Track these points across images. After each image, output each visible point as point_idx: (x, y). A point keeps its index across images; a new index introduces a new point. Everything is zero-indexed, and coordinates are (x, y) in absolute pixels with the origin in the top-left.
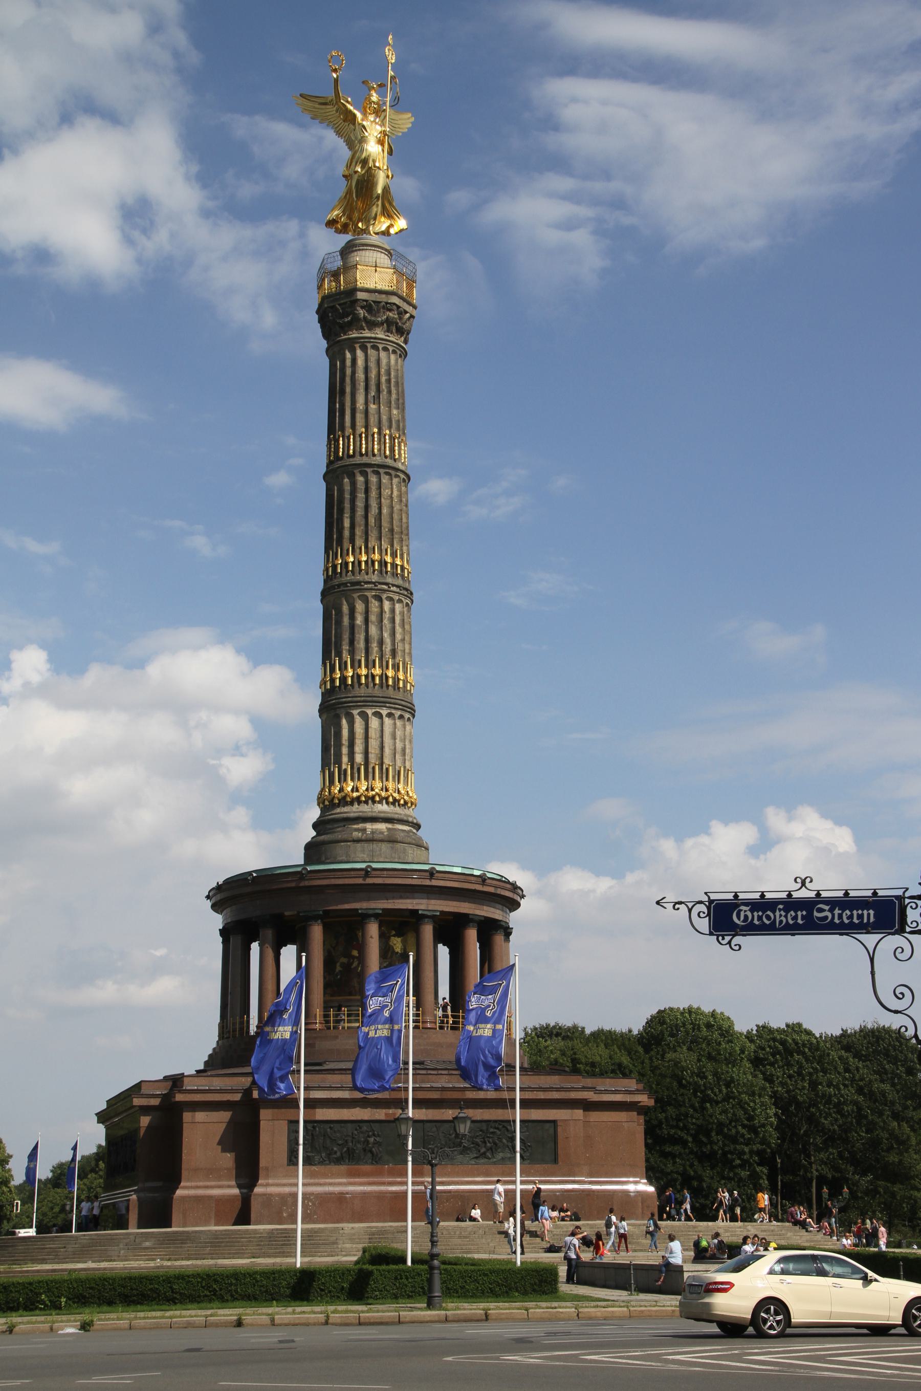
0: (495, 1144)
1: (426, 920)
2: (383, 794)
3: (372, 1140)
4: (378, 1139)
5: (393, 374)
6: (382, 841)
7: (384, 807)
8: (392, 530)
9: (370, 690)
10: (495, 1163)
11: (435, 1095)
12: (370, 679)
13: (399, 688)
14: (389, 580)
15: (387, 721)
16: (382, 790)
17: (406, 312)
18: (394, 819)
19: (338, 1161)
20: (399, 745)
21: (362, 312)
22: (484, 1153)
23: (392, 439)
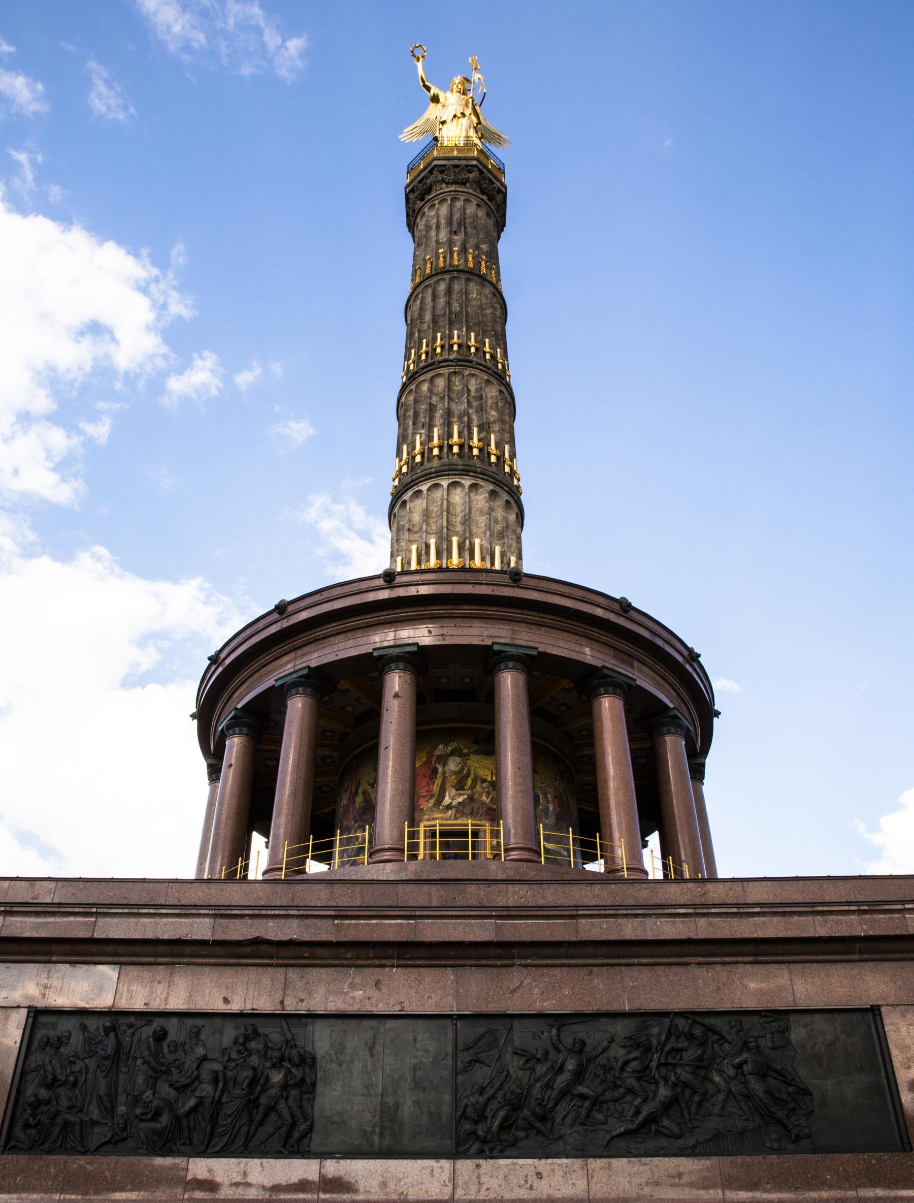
1: (511, 664)
9: (445, 460)
12: (445, 450)
13: (490, 464)
17: (493, 183)
21: (440, 177)
22: (652, 1119)
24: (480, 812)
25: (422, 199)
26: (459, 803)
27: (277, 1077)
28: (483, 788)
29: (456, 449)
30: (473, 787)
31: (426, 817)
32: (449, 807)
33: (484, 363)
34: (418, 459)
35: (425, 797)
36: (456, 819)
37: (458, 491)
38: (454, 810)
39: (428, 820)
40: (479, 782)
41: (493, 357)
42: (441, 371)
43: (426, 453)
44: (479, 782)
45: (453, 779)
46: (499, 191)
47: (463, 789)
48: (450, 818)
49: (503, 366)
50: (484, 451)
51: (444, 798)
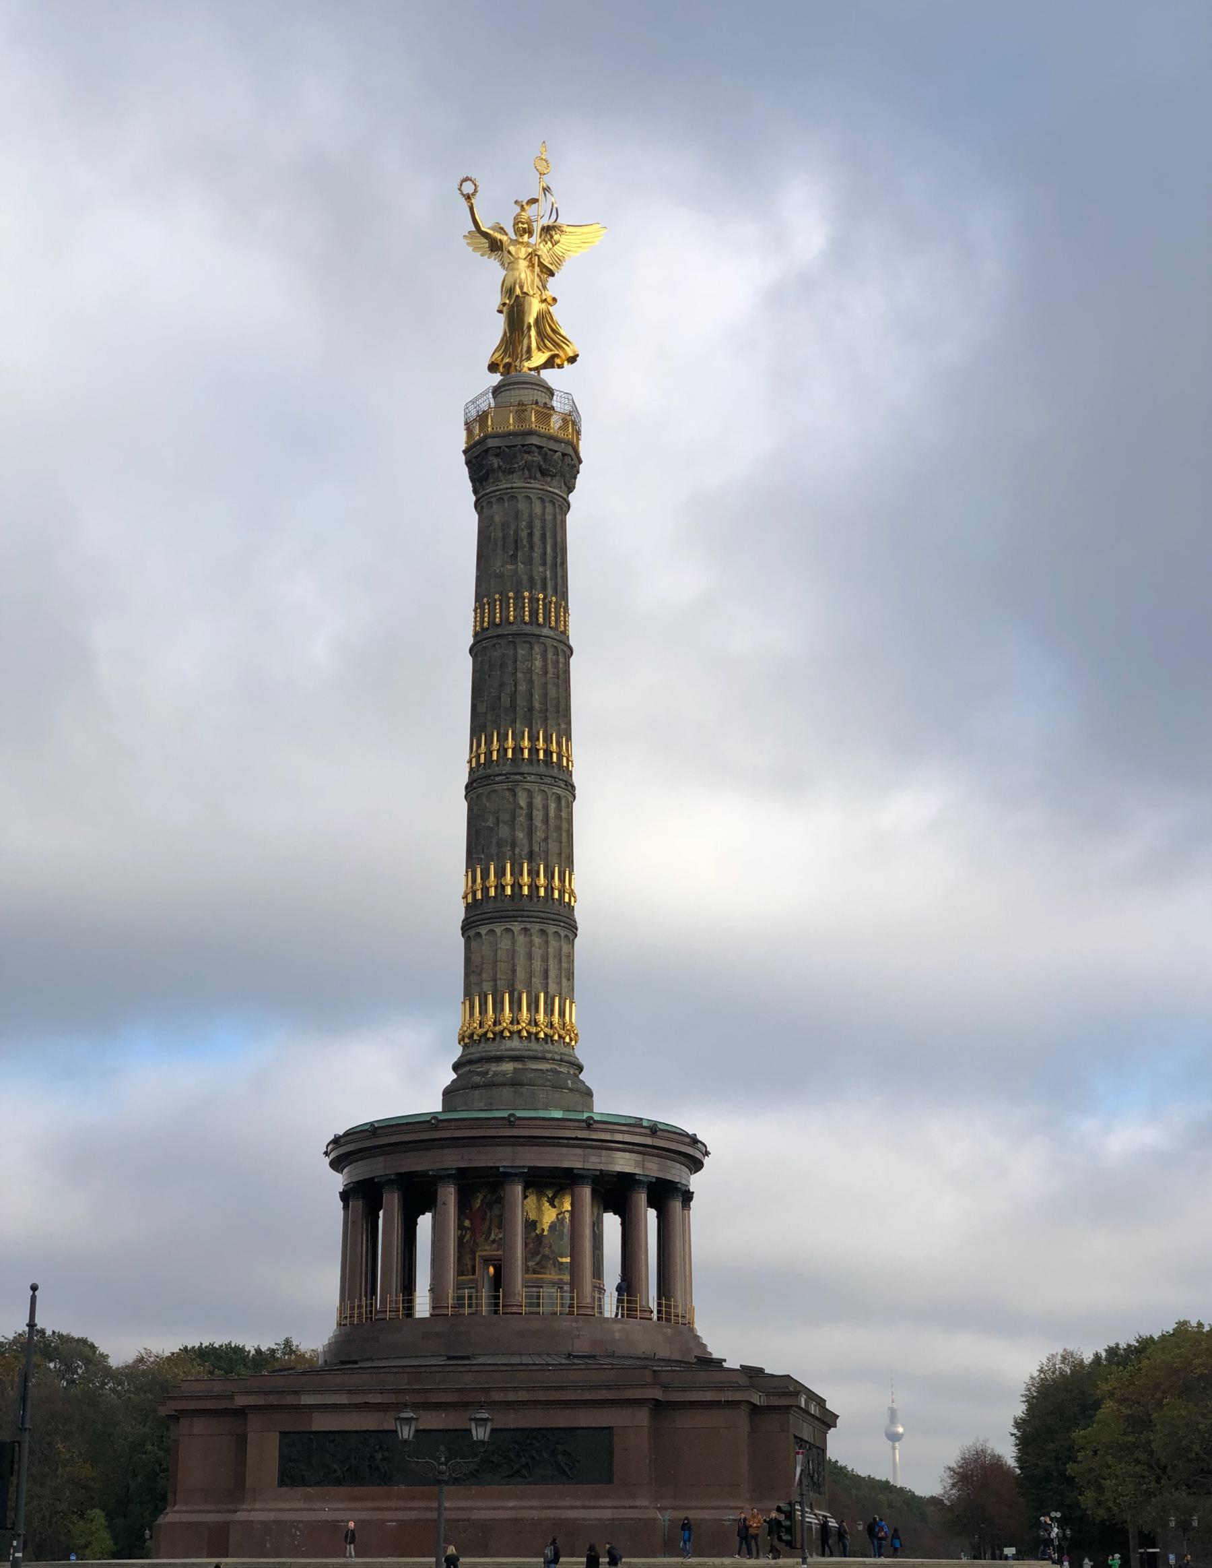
0: (533, 1458)
2: (515, 1028)
3: (379, 1456)
4: (386, 1454)
5: (537, 524)
6: (503, 1085)
7: (516, 1043)
8: (531, 709)
10: (530, 1483)
11: (453, 1398)
14: (525, 769)
15: (521, 939)
16: (512, 1023)
18: (523, 1057)
19: (339, 1482)
20: (537, 965)
21: (496, 462)
23: (533, 600)
25: (481, 483)
27: (379, 1456)
29: (508, 891)
32: (494, 1241)
33: (533, 770)
34: (479, 896)
37: (510, 935)
41: (548, 753)
42: (497, 787)
43: (485, 890)
46: (564, 455)
49: (560, 757)
50: (534, 887)
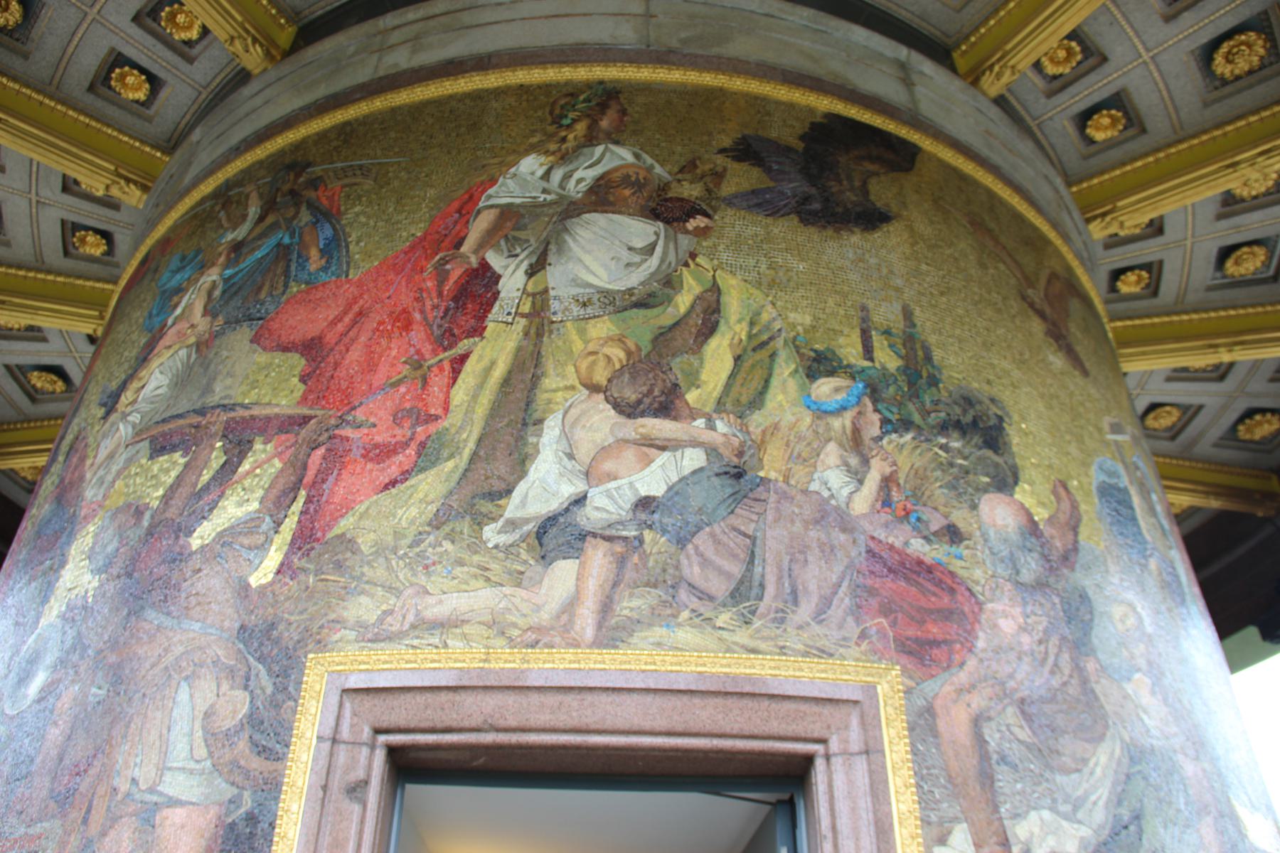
24: (815, 576)
26: (645, 504)
28: (821, 413)
30: (744, 396)
31: (364, 608)
32: (556, 535)
35: (382, 453)
36: (611, 633)
38: (598, 558)
39: (376, 636)
40: (785, 369)
44: (785, 369)
45: (596, 343)
47: (668, 404)
48: (556, 631)
51: (521, 463)
